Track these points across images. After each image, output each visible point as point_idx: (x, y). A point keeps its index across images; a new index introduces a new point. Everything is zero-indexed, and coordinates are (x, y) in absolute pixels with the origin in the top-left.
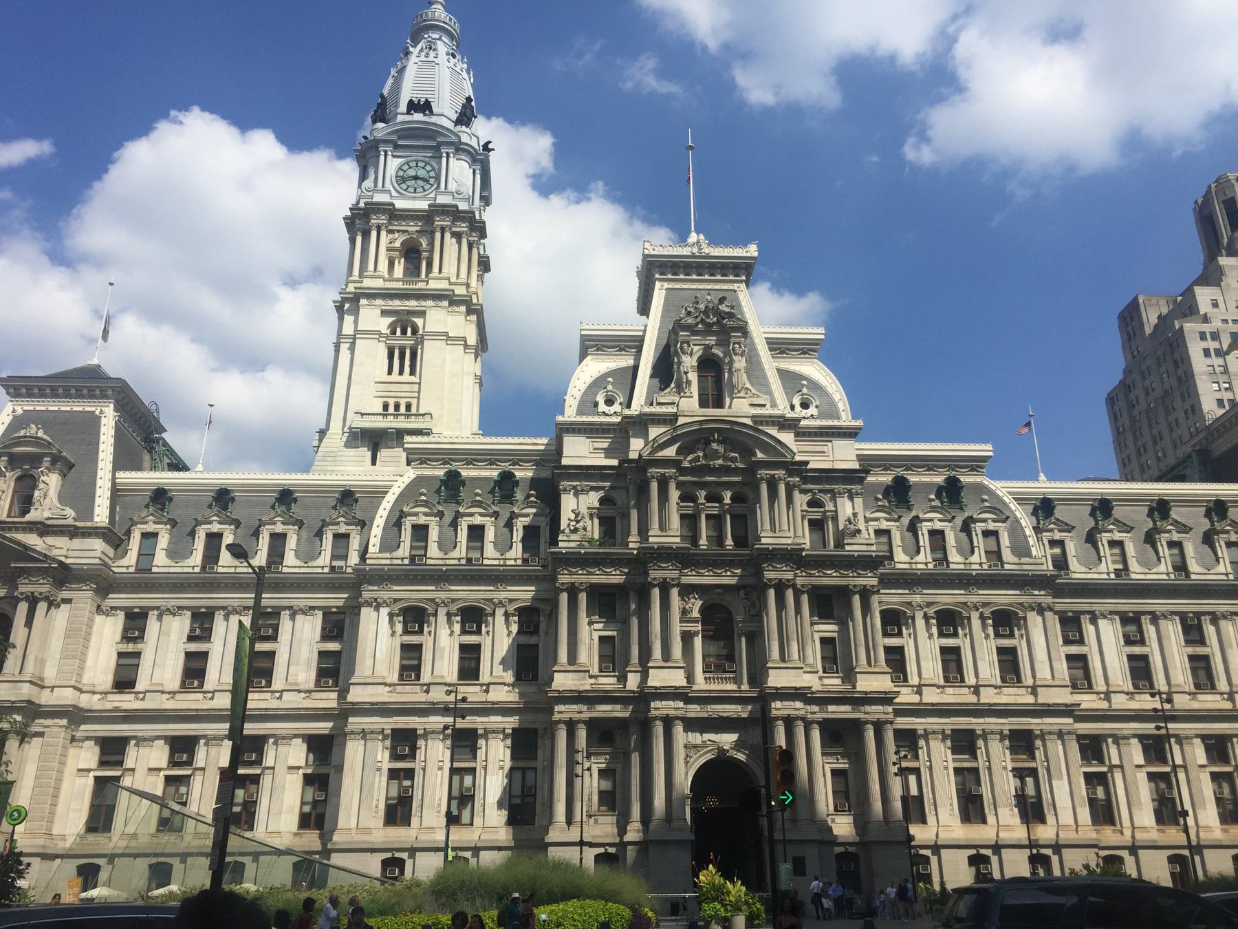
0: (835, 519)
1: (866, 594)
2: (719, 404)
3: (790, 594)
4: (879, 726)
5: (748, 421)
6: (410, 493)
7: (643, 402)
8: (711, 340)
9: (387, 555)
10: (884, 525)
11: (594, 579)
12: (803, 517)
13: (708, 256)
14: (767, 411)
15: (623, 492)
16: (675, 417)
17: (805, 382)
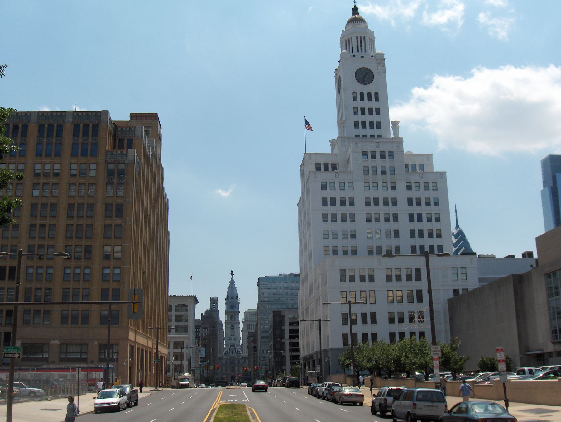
16: (230, 356)
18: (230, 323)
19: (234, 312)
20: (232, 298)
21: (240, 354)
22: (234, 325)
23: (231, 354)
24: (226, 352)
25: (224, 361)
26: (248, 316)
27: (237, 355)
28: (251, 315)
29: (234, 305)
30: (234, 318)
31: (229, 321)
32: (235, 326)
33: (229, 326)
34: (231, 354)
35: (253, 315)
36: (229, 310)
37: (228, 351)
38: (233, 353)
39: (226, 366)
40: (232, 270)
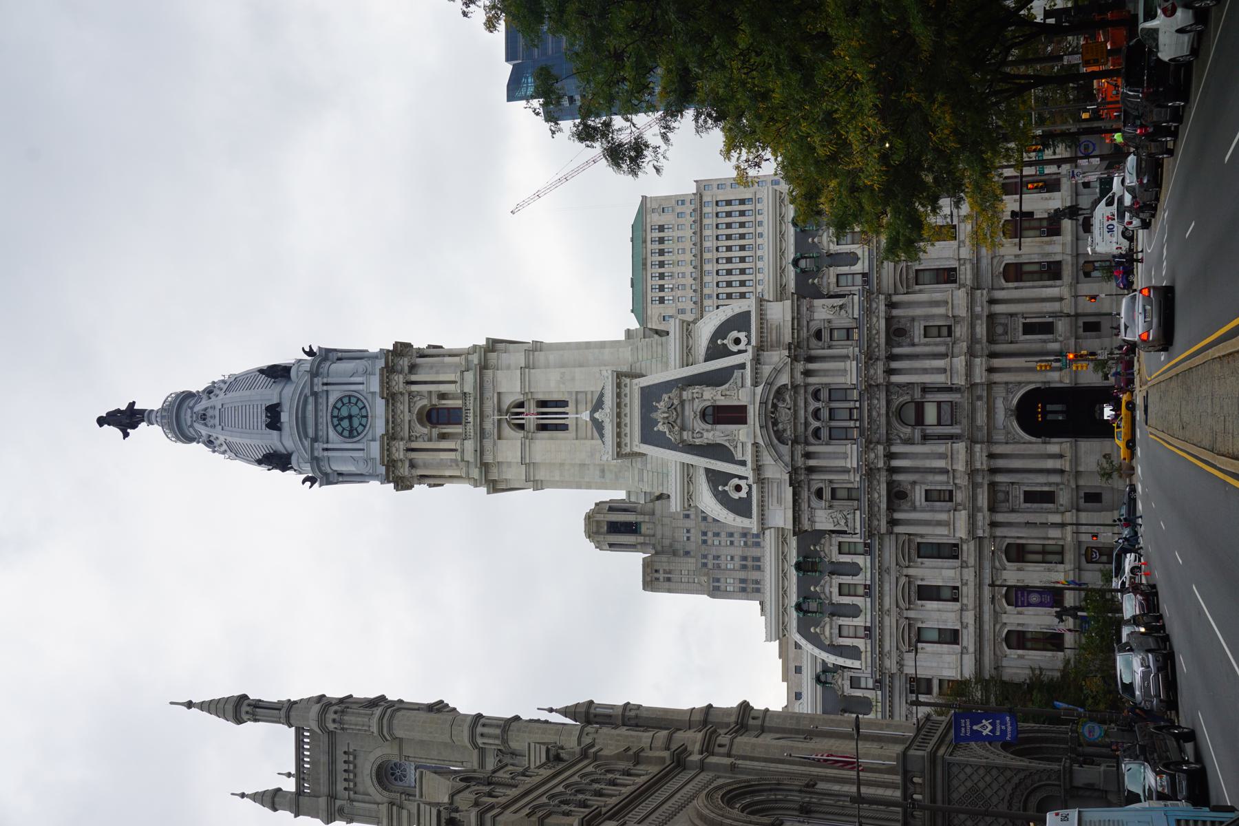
0: (829, 321)
1: (891, 305)
2: (742, 409)
3: (895, 365)
4: (992, 302)
5: (759, 389)
6: (815, 641)
7: (743, 468)
8: (688, 412)
9: (863, 656)
11: (884, 506)
12: (830, 347)
13: (612, 410)
15: (812, 482)
16: (756, 445)
17: (719, 342)
18: (482, 434)
19: (391, 397)
20: (273, 417)
21: (740, 322)
22: (507, 401)
23: (744, 436)
25: (823, 519)
27: (746, 358)
28: (662, 288)
29: (332, 400)
30: (443, 396)
31: (469, 445)
32: (509, 386)
33: (509, 449)
36: (375, 449)
37: (708, 471)
38: (735, 415)
39: (897, 496)
40: (101, 421)
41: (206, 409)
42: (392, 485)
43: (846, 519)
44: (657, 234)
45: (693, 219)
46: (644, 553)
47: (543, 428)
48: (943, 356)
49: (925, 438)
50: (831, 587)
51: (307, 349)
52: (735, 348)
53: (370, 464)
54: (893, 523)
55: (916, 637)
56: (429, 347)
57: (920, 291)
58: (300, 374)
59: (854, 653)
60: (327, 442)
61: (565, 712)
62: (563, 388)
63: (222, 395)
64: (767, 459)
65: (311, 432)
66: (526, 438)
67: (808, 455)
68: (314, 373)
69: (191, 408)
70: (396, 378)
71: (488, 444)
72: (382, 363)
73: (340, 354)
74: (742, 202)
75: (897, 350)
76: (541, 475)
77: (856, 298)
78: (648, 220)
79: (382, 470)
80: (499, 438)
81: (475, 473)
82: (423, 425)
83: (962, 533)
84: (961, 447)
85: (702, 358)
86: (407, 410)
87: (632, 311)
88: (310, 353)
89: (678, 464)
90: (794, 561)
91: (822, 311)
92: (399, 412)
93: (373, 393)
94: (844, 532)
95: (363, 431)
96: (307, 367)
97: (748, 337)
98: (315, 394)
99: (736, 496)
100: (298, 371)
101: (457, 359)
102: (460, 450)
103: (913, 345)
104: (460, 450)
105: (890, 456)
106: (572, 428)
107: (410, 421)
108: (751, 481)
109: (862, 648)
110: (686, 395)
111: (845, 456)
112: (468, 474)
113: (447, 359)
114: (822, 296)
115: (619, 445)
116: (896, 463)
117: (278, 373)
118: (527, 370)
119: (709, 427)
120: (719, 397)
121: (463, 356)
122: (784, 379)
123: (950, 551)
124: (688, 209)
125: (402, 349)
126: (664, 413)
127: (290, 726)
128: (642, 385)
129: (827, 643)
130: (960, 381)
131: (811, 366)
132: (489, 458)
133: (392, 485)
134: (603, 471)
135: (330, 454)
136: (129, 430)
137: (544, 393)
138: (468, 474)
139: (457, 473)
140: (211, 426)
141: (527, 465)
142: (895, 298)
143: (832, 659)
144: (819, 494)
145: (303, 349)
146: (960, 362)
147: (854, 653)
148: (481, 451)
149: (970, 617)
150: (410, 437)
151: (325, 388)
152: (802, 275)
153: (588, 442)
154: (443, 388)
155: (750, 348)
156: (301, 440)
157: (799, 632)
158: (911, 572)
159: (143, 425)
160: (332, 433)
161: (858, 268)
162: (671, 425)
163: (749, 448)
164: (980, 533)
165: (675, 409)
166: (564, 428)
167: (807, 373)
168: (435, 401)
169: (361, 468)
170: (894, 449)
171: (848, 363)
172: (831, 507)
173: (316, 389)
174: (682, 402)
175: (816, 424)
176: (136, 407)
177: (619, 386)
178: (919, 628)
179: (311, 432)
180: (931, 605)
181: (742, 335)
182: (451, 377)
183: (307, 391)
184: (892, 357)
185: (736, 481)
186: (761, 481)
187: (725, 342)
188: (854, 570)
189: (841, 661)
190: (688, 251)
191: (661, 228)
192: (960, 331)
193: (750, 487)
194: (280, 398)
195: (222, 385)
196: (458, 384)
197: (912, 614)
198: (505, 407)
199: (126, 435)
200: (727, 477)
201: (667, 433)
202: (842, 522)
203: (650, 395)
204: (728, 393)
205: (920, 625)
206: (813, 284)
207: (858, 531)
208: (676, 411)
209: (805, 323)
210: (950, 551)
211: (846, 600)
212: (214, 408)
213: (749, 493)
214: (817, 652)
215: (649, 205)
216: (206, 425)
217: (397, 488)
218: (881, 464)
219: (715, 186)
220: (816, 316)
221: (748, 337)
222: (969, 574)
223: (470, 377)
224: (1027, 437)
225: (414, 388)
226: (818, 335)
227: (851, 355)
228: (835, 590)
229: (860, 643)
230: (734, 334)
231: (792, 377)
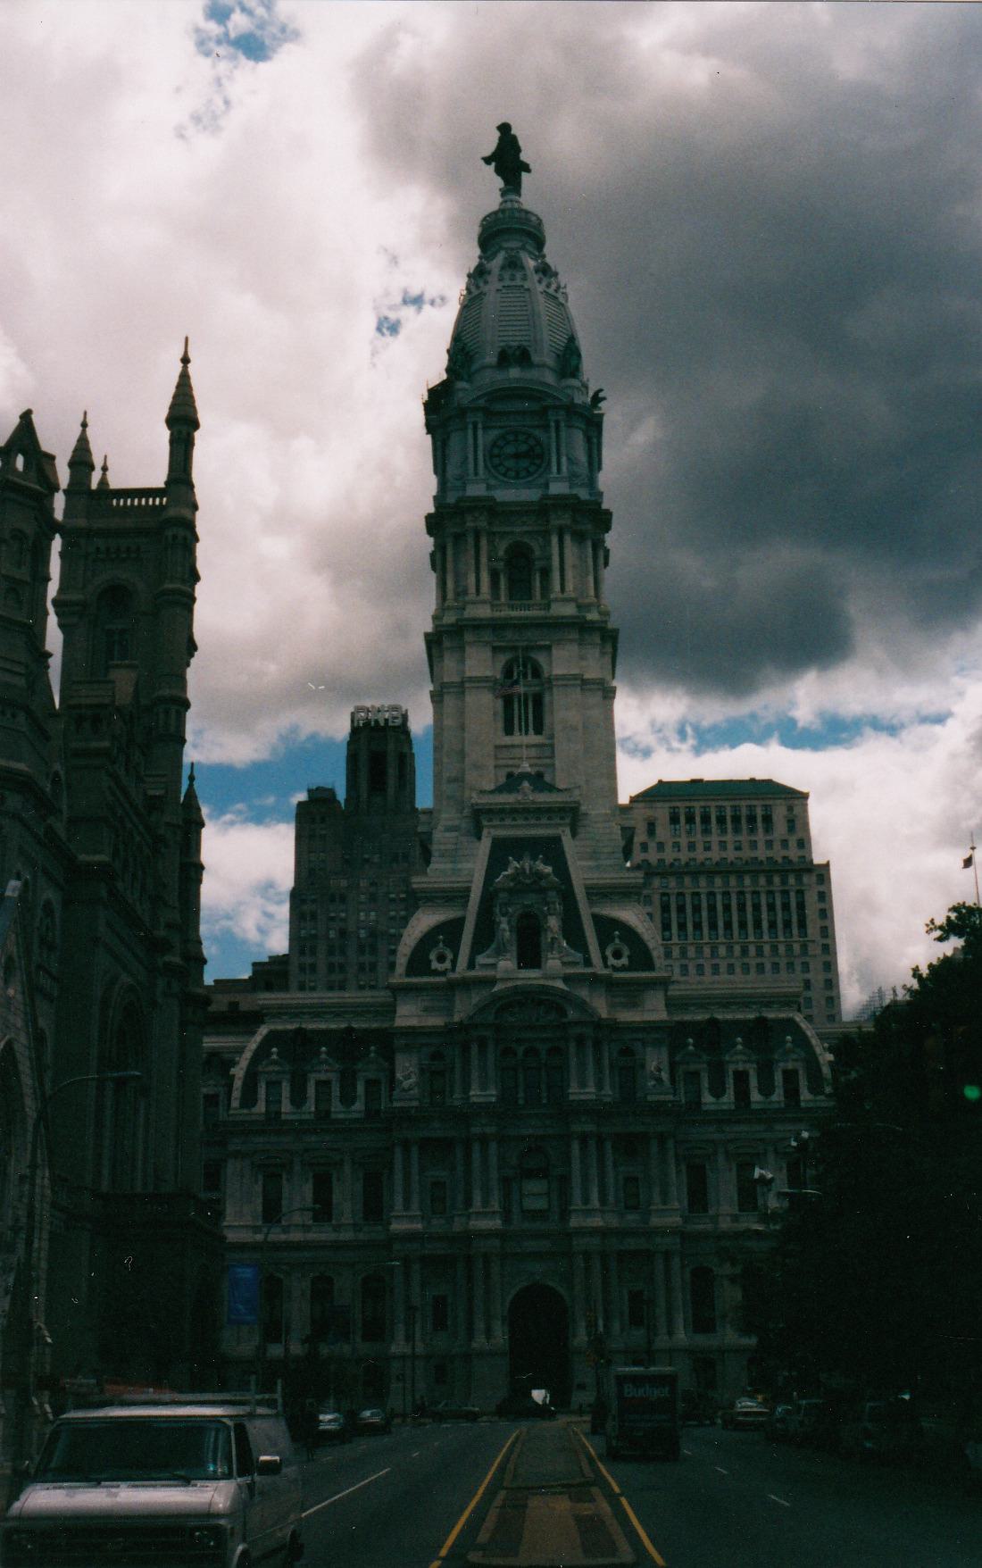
3: (592, 1143)
4: (667, 1255)
5: (560, 984)
6: (261, 1054)
7: (465, 965)
8: (530, 900)
9: (245, 1111)
10: (692, 1067)
12: (612, 1067)
13: (533, 802)
14: (580, 970)
16: (492, 982)
19: (545, 508)
21: (642, 958)
22: (541, 658)
24: (428, 940)
26: (663, 832)
27: (598, 968)
29: (537, 432)
30: (546, 573)
31: (484, 612)
32: (562, 661)
33: (480, 662)
34: (507, 964)
35: (706, 819)
36: (476, 490)
38: (530, 956)
40: (505, 129)
41: (523, 268)
42: (432, 510)
43: (410, 1089)
44: (759, 812)
45: (780, 860)
46: (346, 800)
47: (508, 702)
48: (603, 1201)
49: (505, 1181)
50: (325, 1070)
51: (601, 395)
52: (609, 952)
53: (458, 483)
54: (406, 1145)
55: (272, 1174)
56: (607, 552)
57: (679, 1172)
58: (569, 391)
59: (249, 1098)
60: (485, 428)
61: (191, 794)
62: (558, 728)
63: (541, 288)
64: (476, 998)
65: (498, 407)
66: (496, 681)
67: (482, 1043)
68: (572, 410)
69: (523, 248)
70: (567, 516)
71: (487, 636)
72: (584, 494)
73: (595, 440)
74: (802, 924)
75: (608, 1145)
76: (449, 701)
77: (671, 1097)
78: (778, 802)
79: (451, 499)
80: (495, 650)
81: (450, 619)
82: (506, 552)
83: (396, 1226)
84: (495, 1223)
85: (597, 910)
86: (525, 528)
87: (660, 782)
88: (597, 399)
89: (466, 885)
90: (355, 1026)
91: (655, 1060)
92: (525, 519)
93: (547, 486)
94: (392, 1089)
95: (500, 474)
96: (579, 399)
97: (623, 969)
98: (545, 410)
99: (433, 956)
100: (572, 387)
101: (592, 592)
102: (478, 598)
103: (615, 1166)
104: (478, 598)
105: (484, 1140)
106: (508, 740)
107: (512, 533)
108: (451, 975)
109: (255, 1110)
110: (552, 895)
111: (484, 1087)
112: (449, 608)
113: (591, 579)
114: (671, 1055)
115: (490, 811)
116: (476, 1147)
117: (569, 360)
118: (579, 682)
119: (514, 924)
120: (550, 935)
121: (595, 600)
122: (572, 1014)
123: (374, 1209)
124: (793, 853)
125: (603, 520)
126: (531, 869)
127: (166, 483)
128: (563, 838)
129: (260, 1069)
130: (574, 1222)
131: (589, 1043)
132: (468, 637)
133: (432, 510)
134: (456, 780)
135: (470, 432)
136: (493, 164)
137: (551, 703)
138: (449, 608)
139: (450, 595)
140: (500, 275)
141: (462, 683)
142: (670, 1144)
143: (239, 1072)
144: (437, 1056)
145: (601, 390)
146: (596, 1221)
147: (249, 1098)
148: (478, 626)
149: (296, 1236)
150: (494, 533)
151: (553, 424)
152: (698, 1030)
153: (491, 763)
154: (556, 575)
155: (606, 972)
156: (485, 395)
157: (271, 1032)
158: (347, 1168)
159: (499, 182)
160: (494, 433)
161: (708, 1098)
162: (513, 878)
163: (489, 973)
164: (397, 1246)
165: (535, 882)
166: (509, 730)
167: (580, 1041)
168: (538, 564)
169: (452, 471)
170: (493, 1147)
171: (592, 1090)
172: (422, 1071)
173: (550, 413)
174: (543, 891)
175: (521, 1050)
176: (524, 175)
177: (562, 810)
178: (280, 1176)
179: (498, 407)
180: (308, 1189)
181: (624, 961)
182: (570, 586)
183: (549, 402)
184: (601, 1141)
185: (450, 956)
186: (453, 986)
187: (617, 941)
188: (348, 1099)
189: (238, 1084)
190: (738, 854)
191: (768, 819)
192: (632, 1218)
193: (443, 973)
194: (538, 366)
195: (554, 286)
196: (560, 595)
197: (297, 1168)
198: (533, 655)
199: (487, 160)
200: (454, 944)
201: (506, 873)
202: (406, 1084)
203: (551, 850)
204: (556, 945)
205: (284, 1177)
206: (689, 1044)
207: (396, 1104)
208: (532, 884)
209: (640, 1036)
210: (374, 1209)
211: (311, 1091)
212: (525, 278)
213: (436, 973)
214: (248, 1055)
215: (796, 802)
216: (503, 268)
217: (429, 518)
218: (476, 1130)
219: (821, 888)
220: (649, 1049)
221: (623, 969)
222: (346, 1235)
223: (569, 610)
224: (510, 1297)
225: (555, 540)
226: (627, 1052)
227: (603, 1092)
228: (323, 1077)
229: (261, 1107)
230: (626, 952)
231: (577, 1023)
